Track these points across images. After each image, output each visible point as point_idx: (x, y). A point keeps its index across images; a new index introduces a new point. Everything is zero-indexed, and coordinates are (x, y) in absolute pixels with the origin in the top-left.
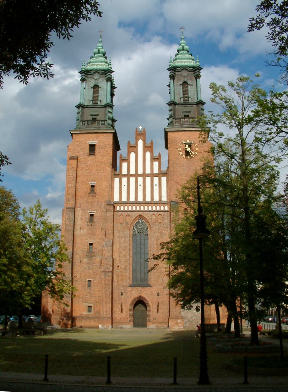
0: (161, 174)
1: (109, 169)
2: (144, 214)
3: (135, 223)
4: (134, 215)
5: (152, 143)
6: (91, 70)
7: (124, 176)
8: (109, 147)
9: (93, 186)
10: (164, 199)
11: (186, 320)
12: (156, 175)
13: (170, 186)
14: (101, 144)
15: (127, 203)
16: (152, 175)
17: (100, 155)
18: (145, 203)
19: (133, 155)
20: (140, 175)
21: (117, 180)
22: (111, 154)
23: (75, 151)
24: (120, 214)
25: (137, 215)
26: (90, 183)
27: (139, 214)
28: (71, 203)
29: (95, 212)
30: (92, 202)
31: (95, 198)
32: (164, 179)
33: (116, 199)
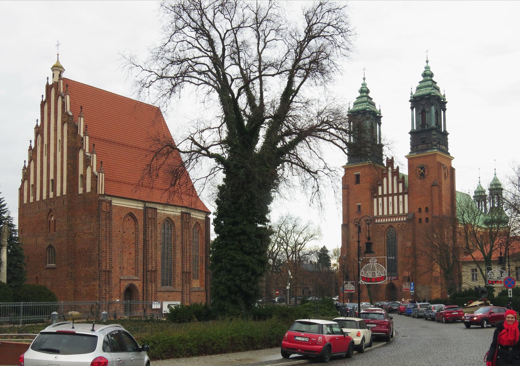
0: (403, 194)
1: (369, 193)
4: (387, 225)
5: (398, 167)
6: (355, 112)
7: (380, 196)
9: (359, 206)
10: (406, 211)
12: (401, 194)
15: (383, 217)
16: (398, 194)
18: (393, 216)
19: (385, 180)
20: (391, 195)
27: (389, 224)
33: (375, 214)
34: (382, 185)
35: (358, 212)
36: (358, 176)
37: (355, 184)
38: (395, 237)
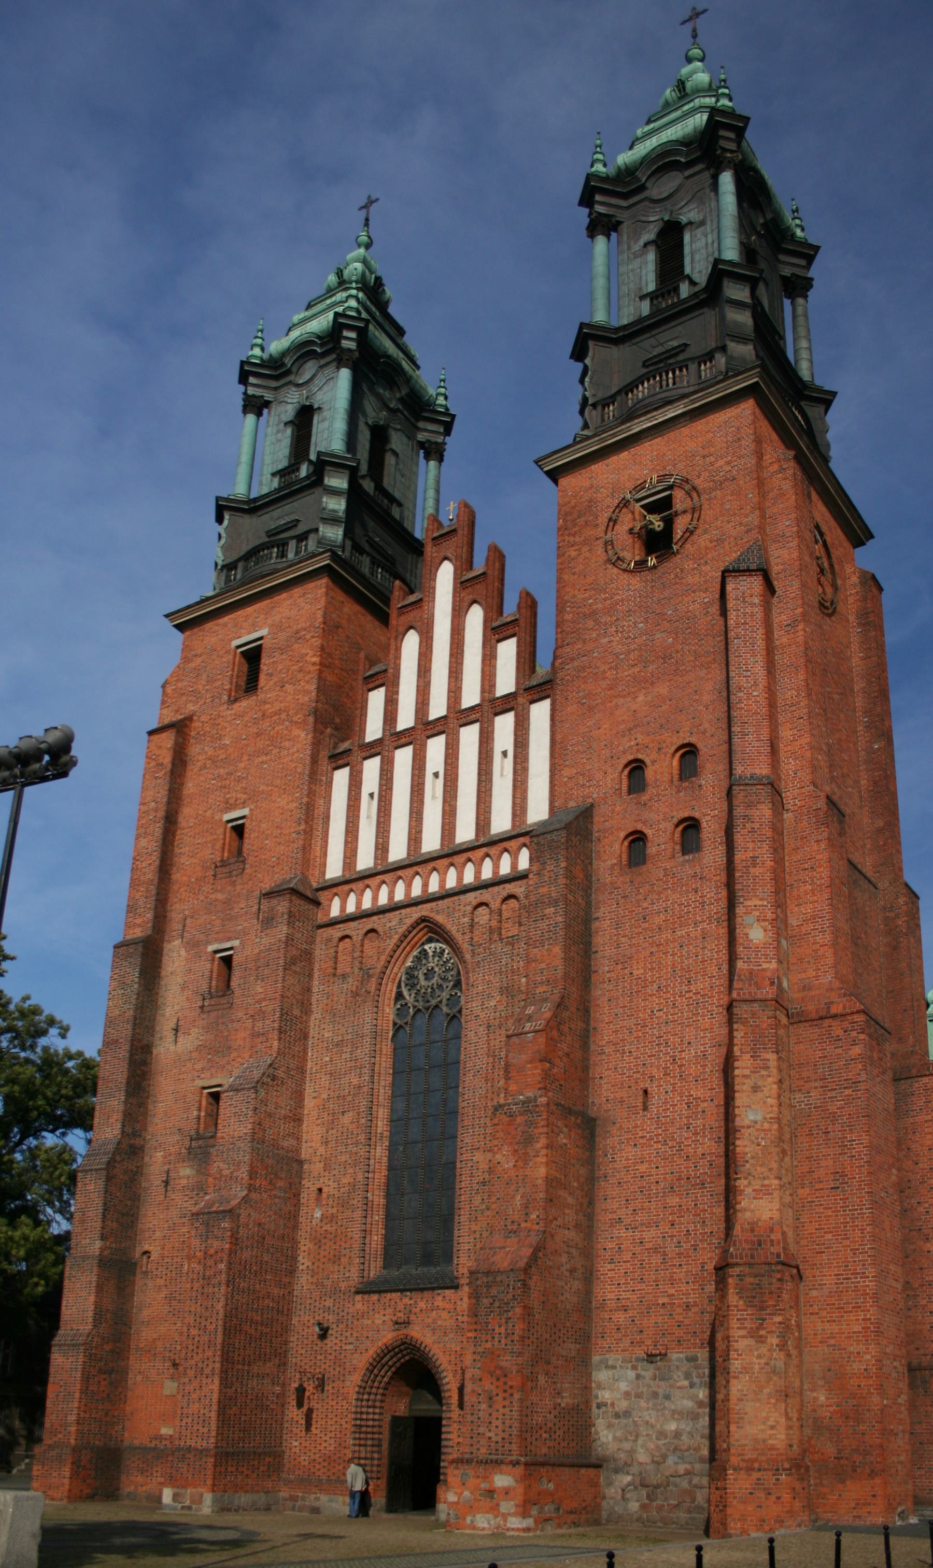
2: (439, 914)
3: (409, 964)
7: (373, 750)
8: (308, 637)
9: (239, 830)
10: (538, 810)
11: (629, 1478)
13: (558, 737)
14: (283, 636)
17: (271, 683)
19: (411, 643)
21: (341, 778)
22: (314, 664)
23: (184, 698)
24: (340, 934)
25: (409, 922)
26: (227, 817)
27: (415, 913)
28: (138, 921)
29: (236, 943)
30: (227, 902)
31: (239, 880)
32: (540, 713)
34: (388, 679)
35: (224, 863)
36: (252, 656)
37: (233, 701)
38: (453, 1000)
